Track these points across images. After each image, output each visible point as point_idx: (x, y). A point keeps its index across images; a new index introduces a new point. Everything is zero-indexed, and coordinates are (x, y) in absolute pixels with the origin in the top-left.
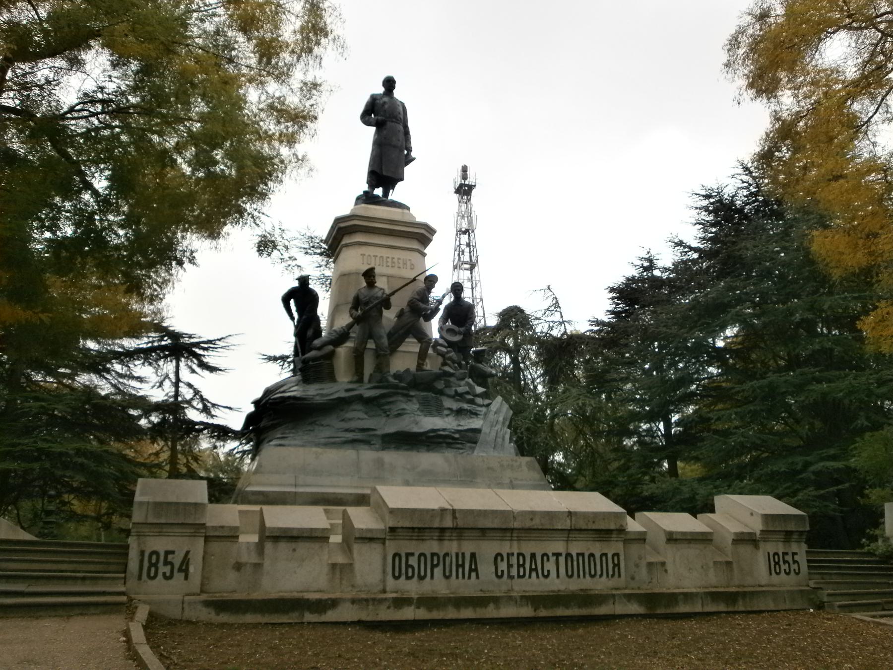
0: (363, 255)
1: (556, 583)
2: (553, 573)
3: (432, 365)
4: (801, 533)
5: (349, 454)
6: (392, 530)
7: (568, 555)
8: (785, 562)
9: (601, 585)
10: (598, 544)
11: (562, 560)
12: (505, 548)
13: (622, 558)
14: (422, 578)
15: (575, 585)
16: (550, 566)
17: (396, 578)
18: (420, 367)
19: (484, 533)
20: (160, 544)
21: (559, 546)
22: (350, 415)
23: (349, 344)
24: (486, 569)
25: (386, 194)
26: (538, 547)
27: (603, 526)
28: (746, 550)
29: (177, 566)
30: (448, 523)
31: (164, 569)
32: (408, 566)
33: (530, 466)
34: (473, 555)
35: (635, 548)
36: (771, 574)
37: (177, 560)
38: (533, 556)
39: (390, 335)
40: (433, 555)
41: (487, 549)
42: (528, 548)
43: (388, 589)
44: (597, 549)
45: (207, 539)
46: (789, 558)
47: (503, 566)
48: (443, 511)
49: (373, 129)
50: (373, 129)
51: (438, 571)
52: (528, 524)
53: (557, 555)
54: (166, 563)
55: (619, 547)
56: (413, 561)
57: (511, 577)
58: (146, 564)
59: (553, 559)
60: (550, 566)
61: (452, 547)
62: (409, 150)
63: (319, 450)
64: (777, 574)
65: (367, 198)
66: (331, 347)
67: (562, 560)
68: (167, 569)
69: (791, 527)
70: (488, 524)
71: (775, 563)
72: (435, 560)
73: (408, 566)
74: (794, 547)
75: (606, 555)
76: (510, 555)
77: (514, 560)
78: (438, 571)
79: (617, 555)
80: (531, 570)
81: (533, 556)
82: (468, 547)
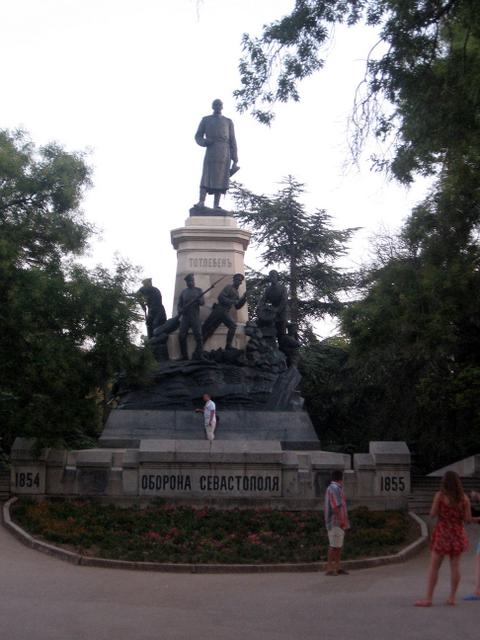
0: (191, 259)
1: (236, 493)
2: (236, 488)
3: (239, 344)
4: (405, 465)
5: (170, 414)
6: (141, 463)
7: (246, 477)
8: (393, 483)
9: (267, 493)
10: (265, 472)
11: (241, 480)
12: (206, 473)
13: (280, 479)
14: (158, 488)
15: (248, 494)
16: (234, 483)
17: (144, 488)
18: (228, 346)
19: (194, 464)
20: (25, 470)
21: (240, 473)
22: (172, 386)
23: (178, 331)
24: (195, 485)
25: (217, 201)
26: (227, 473)
27: (267, 461)
28: (367, 475)
29: (33, 479)
30: (170, 459)
31: (27, 482)
32: (150, 482)
33: (303, 420)
34: (188, 477)
35: (290, 476)
36: (382, 489)
37: (33, 478)
38: (224, 478)
39: (208, 321)
40: (165, 477)
41: (196, 474)
42: (221, 473)
43: (140, 494)
44: (264, 474)
45: (47, 467)
46: (397, 481)
47: (205, 483)
48: (170, 453)
49: (205, 149)
50: (205, 149)
51: (167, 485)
52: (219, 460)
53: (239, 478)
54: (29, 479)
55: (278, 473)
56: (154, 480)
57: (209, 489)
58: (19, 479)
59: (236, 480)
60: (234, 483)
61: (176, 472)
62: (236, 161)
63: (148, 412)
64: (388, 490)
65: (198, 210)
66: (165, 334)
67: (241, 480)
68: (29, 482)
69: (397, 461)
70: (193, 459)
71: (387, 484)
72: (166, 479)
73: (150, 482)
74: (402, 474)
75: (270, 478)
76: (210, 477)
77: (212, 480)
78: (167, 485)
79: (277, 478)
80: (222, 486)
81: (224, 478)
82: (185, 473)
